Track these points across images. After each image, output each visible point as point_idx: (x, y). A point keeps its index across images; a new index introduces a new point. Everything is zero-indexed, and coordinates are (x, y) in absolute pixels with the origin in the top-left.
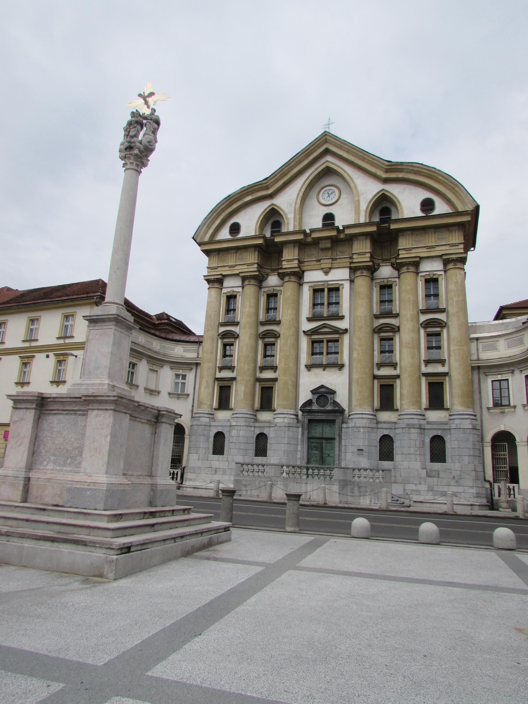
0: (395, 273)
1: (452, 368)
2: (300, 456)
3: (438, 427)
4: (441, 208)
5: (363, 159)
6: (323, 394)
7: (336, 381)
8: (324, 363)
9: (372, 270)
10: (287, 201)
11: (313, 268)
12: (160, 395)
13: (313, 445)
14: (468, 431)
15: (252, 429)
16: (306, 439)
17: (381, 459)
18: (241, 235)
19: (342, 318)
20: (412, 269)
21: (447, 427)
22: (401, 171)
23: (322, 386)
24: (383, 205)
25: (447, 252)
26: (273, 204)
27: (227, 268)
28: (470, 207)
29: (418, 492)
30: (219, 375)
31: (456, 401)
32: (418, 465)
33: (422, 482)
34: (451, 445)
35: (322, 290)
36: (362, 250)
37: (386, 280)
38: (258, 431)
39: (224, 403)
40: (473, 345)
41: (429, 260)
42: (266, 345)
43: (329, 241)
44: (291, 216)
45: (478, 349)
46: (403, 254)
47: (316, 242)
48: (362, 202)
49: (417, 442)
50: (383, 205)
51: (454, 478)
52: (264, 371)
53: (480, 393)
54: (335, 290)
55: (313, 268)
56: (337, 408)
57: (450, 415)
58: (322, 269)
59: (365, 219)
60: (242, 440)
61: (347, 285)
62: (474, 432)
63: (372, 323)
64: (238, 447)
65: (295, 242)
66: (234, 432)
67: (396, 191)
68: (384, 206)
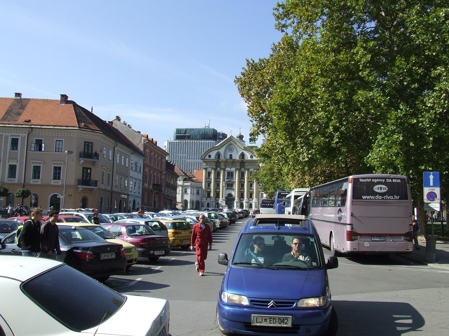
10: (222, 151)
24: (243, 155)
42: (217, 184)
46: (246, 168)
67: (245, 152)
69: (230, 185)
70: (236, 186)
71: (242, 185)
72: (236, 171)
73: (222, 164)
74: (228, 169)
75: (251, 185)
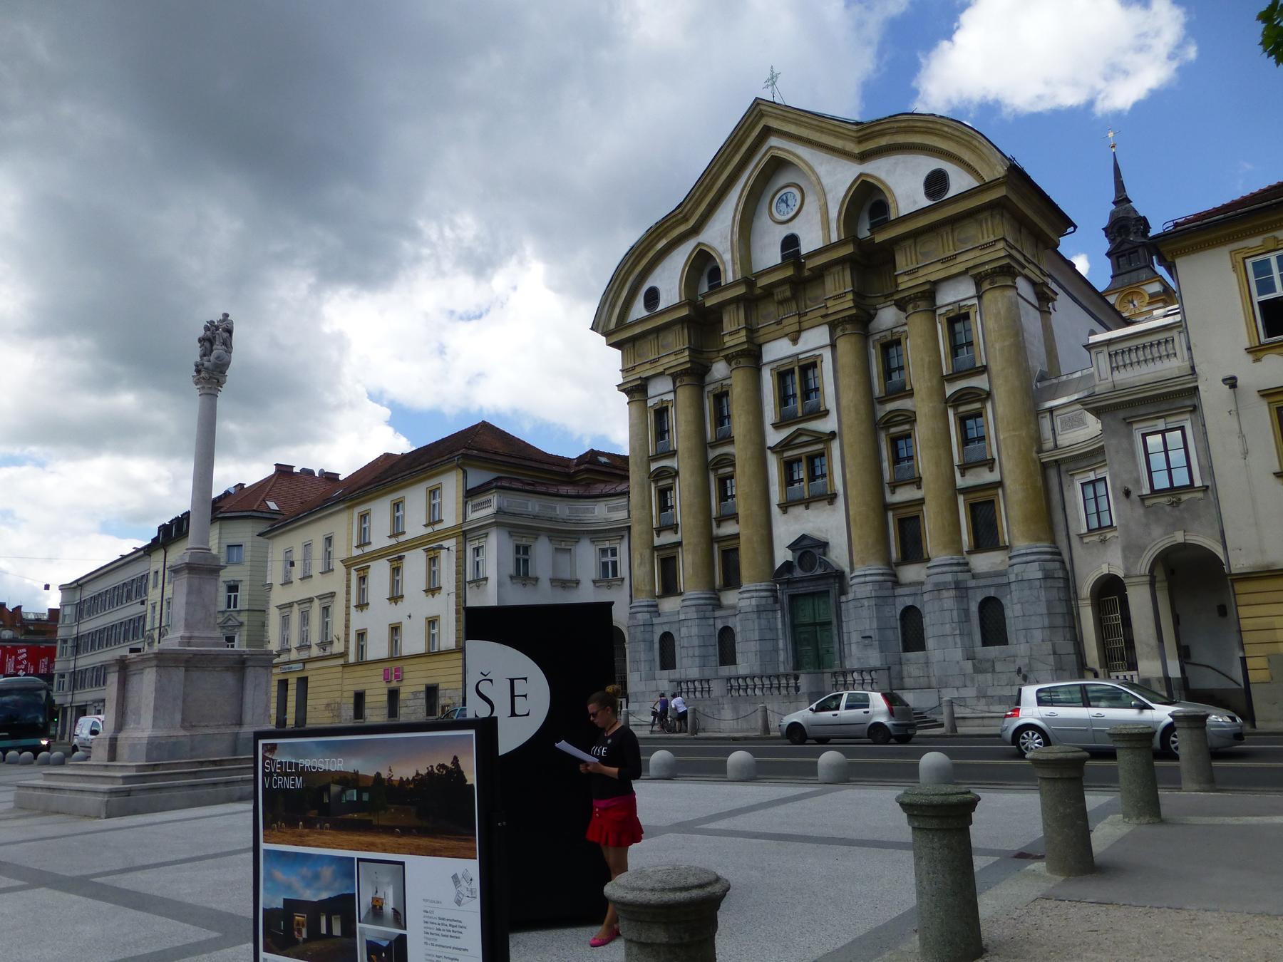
0: (903, 315)
1: (1006, 472)
2: (783, 659)
3: (989, 581)
4: (959, 182)
5: (821, 130)
6: (809, 549)
7: (827, 523)
8: (806, 496)
9: (861, 320)
10: (719, 234)
11: (771, 336)
12: (581, 586)
13: (802, 636)
14: (1037, 583)
15: (711, 622)
16: (788, 630)
17: (906, 649)
18: (662, 306)
19: (826, 413)
20: (923, 305)
21: (1005, 580)
22: (882, 134)
23: (803, 537)
24: (868, 200)
25: (978, 261)
26: (699, 244)
27: (648, 366)
28: (1000, 171)
29: (962, 701)
30: (658, 541)
31: (1016, 530)
32: (958, 654)
33: (968, 683)
34: (1013, 611)
35: (792, 371)
36: (838, 292)
37: (888, 333)
38: (720, 625)
39: (670, 587)
40: (1046, 423)
41: (951, 282)
43: (787, 287)
44: (727, 257)
45: (1053, 429)
46: (905, 283)
47: (769, 291)
48: (830, 205)
49: (955, 613)
50: (868, 200)
51: (1019, 671)
52: (723, 524)
53: (1064, 509)
54: (809, 366)
55: (771, 336)
56: (829, 571)
57: (1010, 558)
58: (786, 335)
59: (839, 235)
60: (696, 642)
61: (827, 355)
62: (1049, 583)
63: (872, 412)
64: (691, 653)
65: (736, 300)
66: (684, 631)
68: (875, 199)
69: (805, 469)
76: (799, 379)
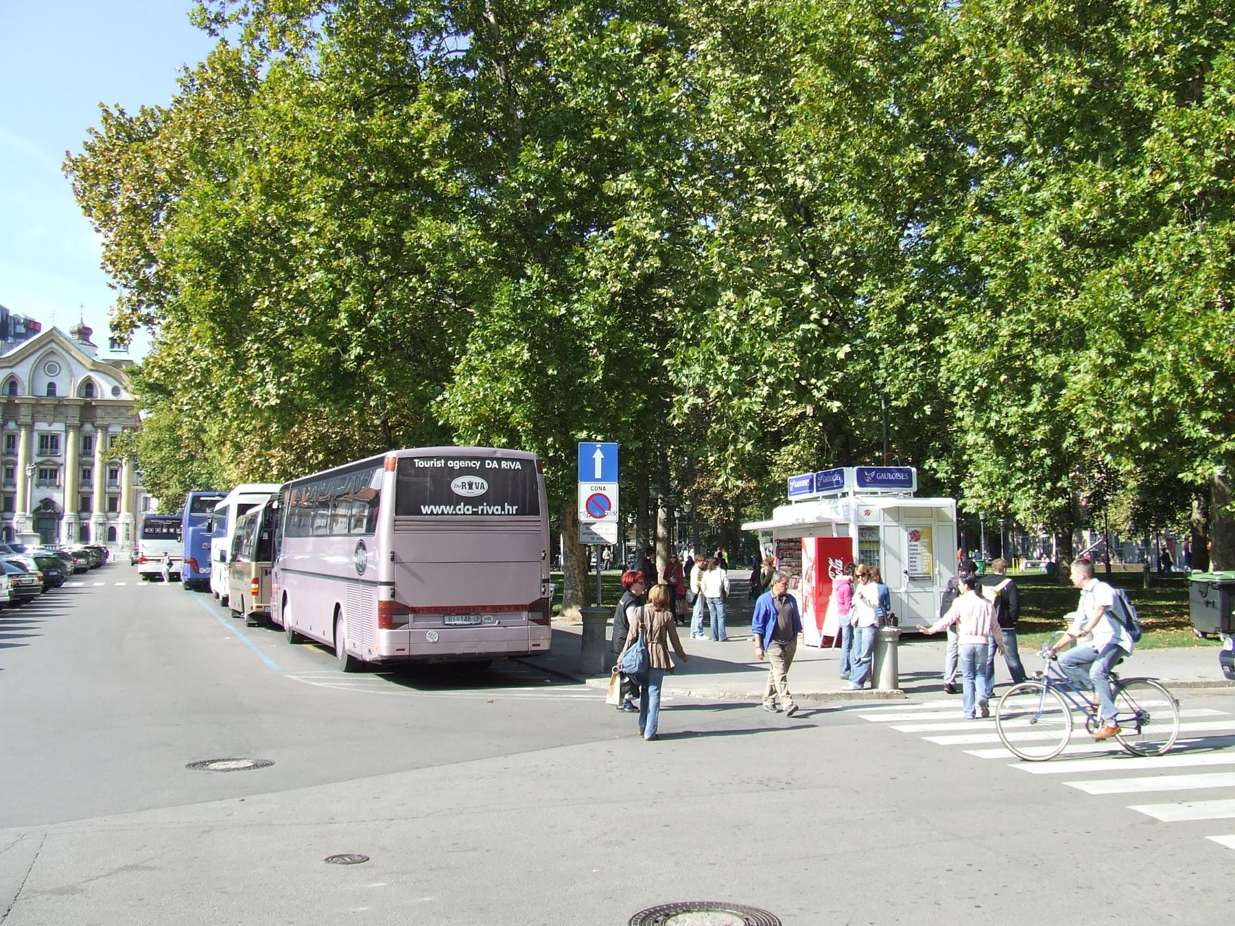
42: (8, 470)
44: (26, 384)
61: (63, 435)
67: (97, 378)
69: (47, 475)
70: (67, 477)
71: (85, 474)
72: (67, 432)
73: (23, 410)
74: (42, 426)
75: (114, 474)
76: (50, 443)
